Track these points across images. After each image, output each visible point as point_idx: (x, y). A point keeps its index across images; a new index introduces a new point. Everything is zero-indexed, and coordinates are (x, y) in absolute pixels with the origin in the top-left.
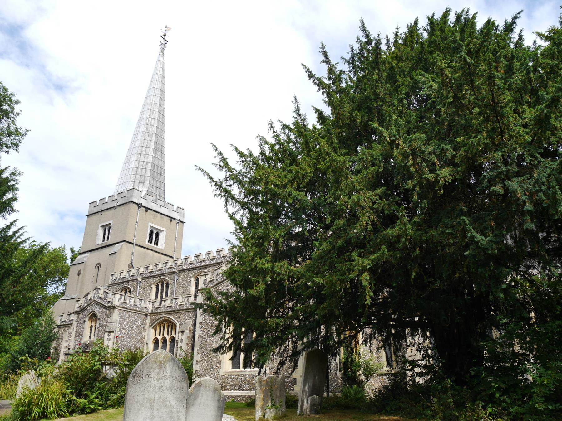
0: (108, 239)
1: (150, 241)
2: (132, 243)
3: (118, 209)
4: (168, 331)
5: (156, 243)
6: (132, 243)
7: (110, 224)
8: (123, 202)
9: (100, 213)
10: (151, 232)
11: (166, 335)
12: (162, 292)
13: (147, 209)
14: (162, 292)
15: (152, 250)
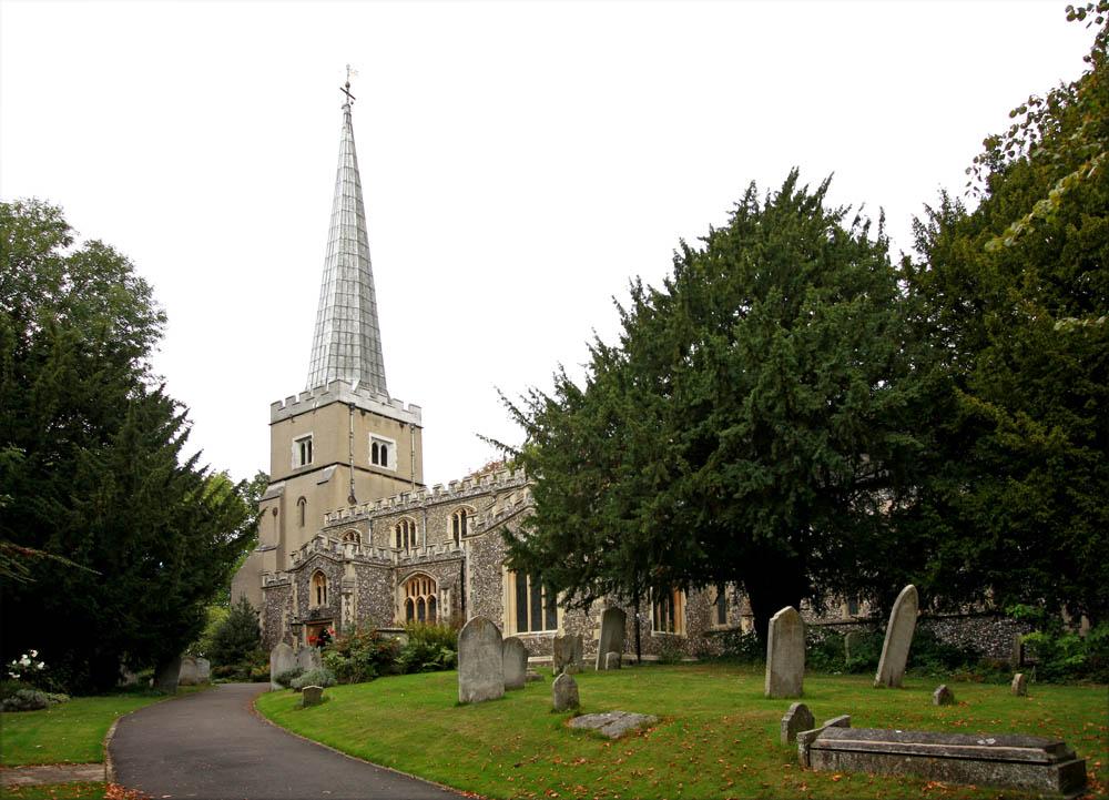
0: (310, 460)
1: (375, 460)
2: (348, 466)
3: (319, 412)
4: (424, 589)
5: (384, 463)
6: (348, 466)
7: (310, 437)
8: (326, 402)
9: (290, 421)
10: (375, 447)
11: (422, 595)
12: (406, 536)
13: (364, 411)
14: (406, 536)
15: (380, 474)
